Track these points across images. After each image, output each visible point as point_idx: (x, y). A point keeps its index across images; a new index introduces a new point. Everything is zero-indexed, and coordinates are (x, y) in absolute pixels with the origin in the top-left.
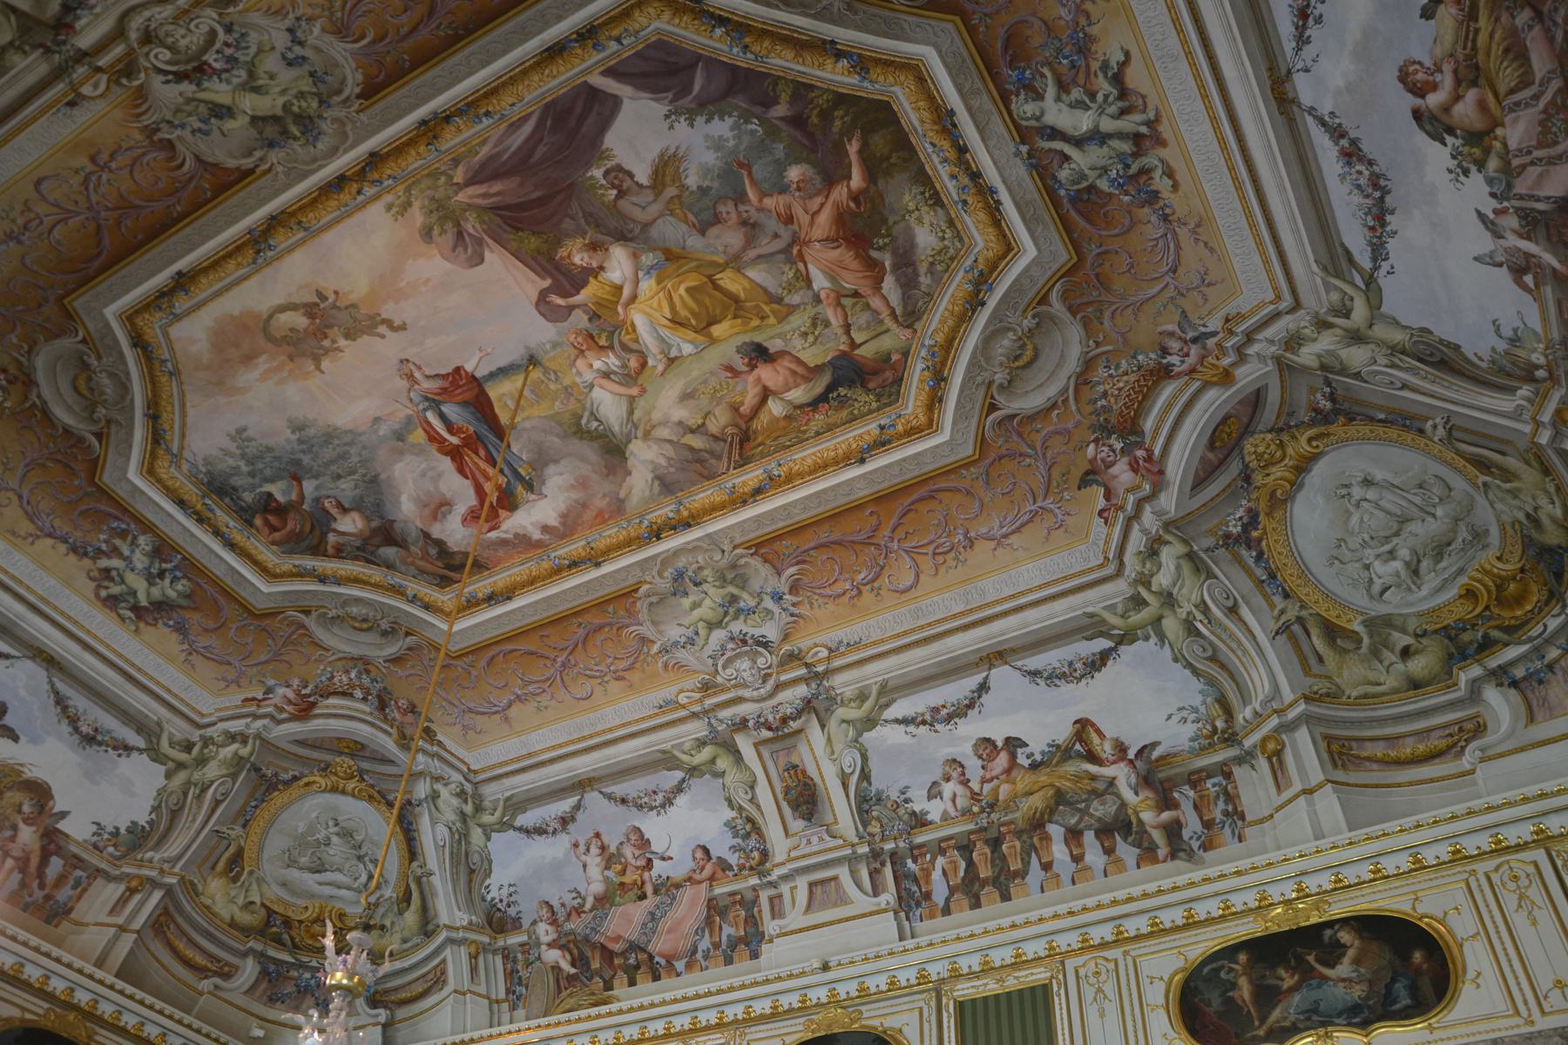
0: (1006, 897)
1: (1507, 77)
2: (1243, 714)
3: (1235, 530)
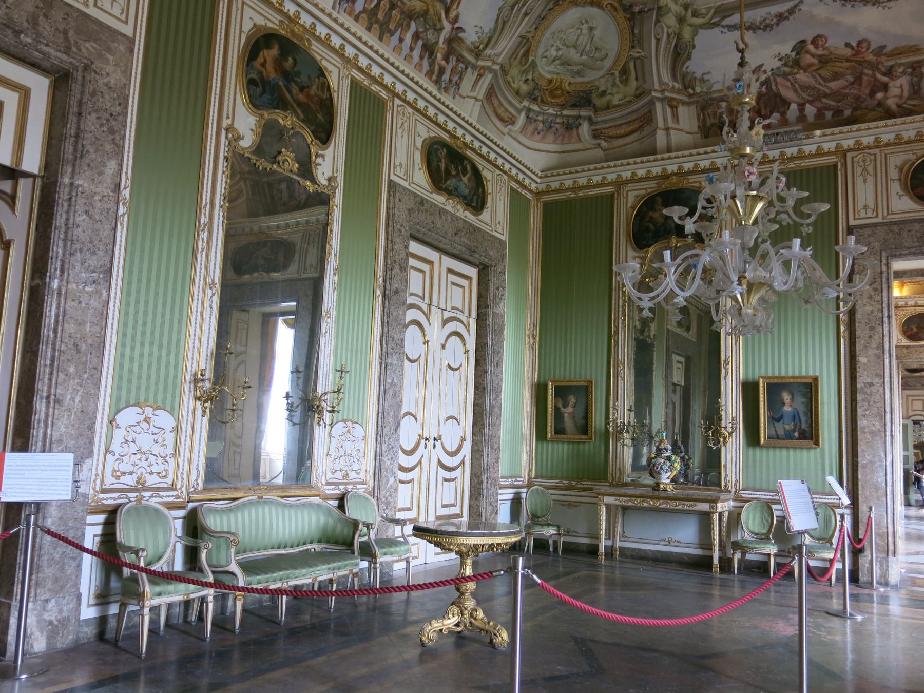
0: (381, 39)
2: (488, 52)
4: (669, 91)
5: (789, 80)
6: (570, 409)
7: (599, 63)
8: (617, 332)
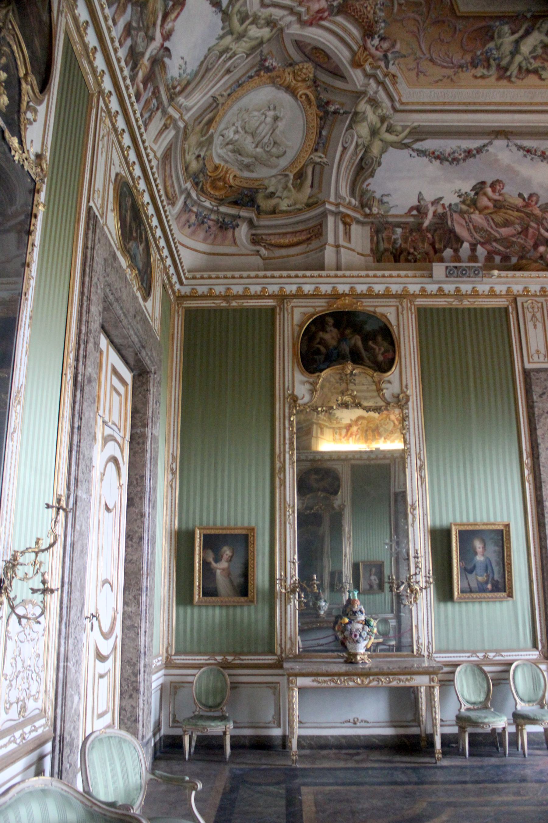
1: (498, 219)
3: (267, 64)
4: (344, 206)
5: (464, 218)
6: (223, 564)
7: (274, 160)
8: (283, 469)
